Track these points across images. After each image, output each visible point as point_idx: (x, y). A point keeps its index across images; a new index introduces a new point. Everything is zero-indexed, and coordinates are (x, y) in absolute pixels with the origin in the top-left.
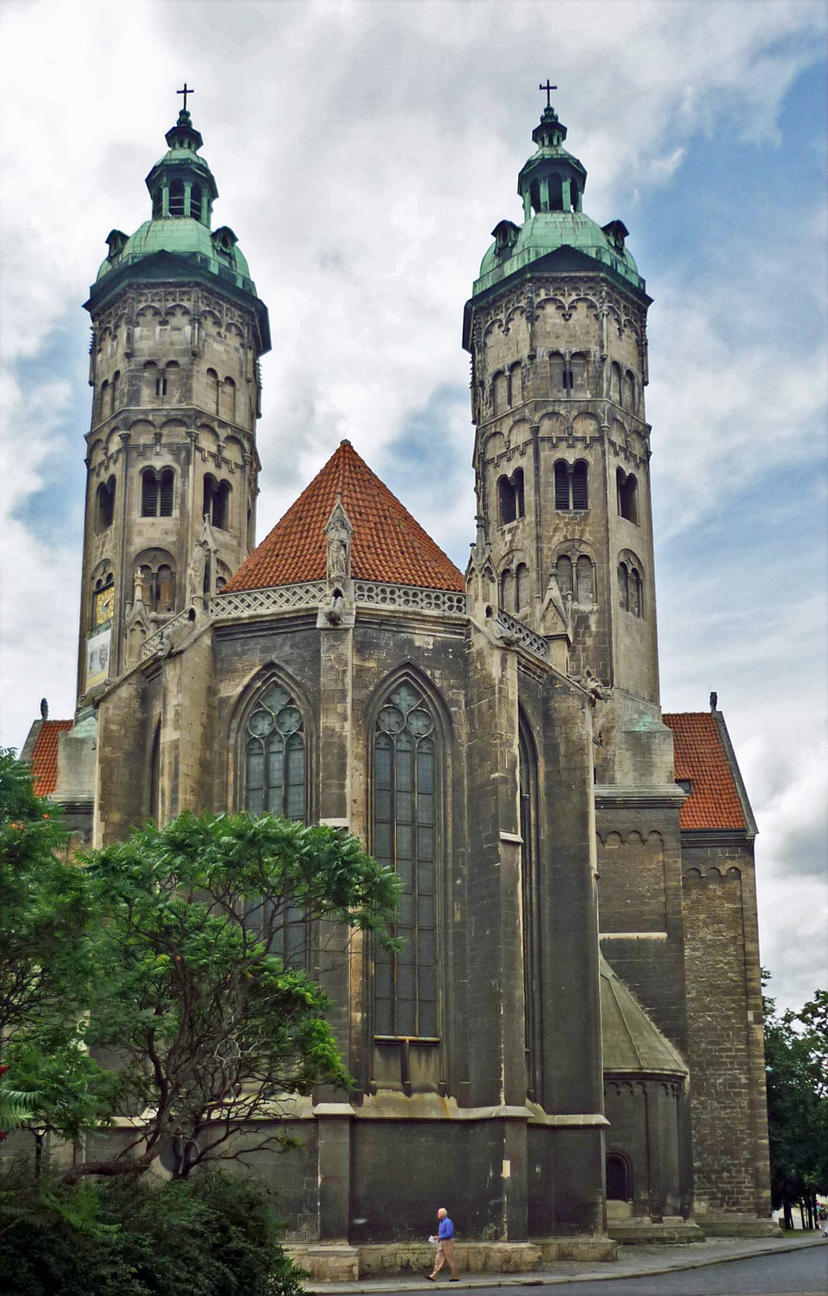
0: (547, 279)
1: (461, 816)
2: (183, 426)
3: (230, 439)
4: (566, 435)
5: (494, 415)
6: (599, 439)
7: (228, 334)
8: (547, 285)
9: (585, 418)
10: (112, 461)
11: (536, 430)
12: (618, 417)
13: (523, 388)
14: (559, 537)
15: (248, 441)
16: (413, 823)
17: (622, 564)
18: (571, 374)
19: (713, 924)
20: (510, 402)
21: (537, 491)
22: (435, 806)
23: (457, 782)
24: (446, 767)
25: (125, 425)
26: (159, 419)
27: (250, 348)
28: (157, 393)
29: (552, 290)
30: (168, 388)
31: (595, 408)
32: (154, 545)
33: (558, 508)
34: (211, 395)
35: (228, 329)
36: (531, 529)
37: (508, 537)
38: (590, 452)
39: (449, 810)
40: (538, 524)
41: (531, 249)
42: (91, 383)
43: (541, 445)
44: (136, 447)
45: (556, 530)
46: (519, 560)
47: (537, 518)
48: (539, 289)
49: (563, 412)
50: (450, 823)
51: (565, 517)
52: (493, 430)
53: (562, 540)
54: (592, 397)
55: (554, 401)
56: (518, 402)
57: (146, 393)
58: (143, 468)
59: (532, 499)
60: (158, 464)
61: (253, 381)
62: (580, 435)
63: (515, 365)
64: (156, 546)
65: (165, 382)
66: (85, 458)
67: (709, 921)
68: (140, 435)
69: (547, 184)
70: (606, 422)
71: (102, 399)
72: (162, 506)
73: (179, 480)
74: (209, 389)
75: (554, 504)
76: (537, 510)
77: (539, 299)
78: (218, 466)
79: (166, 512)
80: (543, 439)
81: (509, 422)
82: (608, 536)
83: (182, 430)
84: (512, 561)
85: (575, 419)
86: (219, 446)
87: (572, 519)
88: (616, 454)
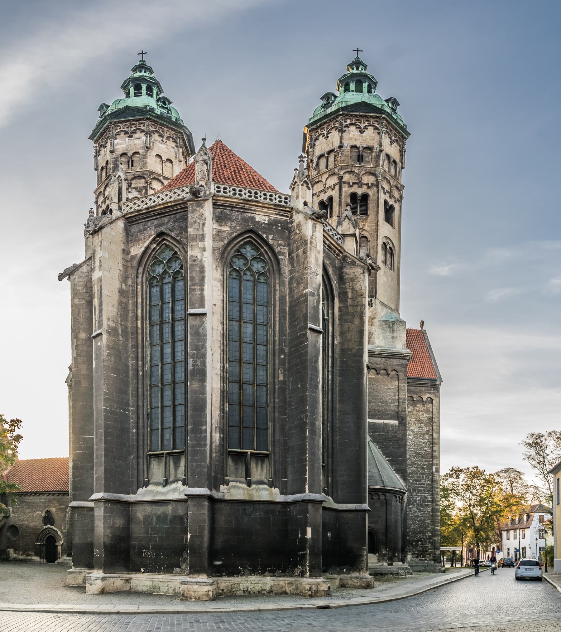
0: (352, 115)
1: (284, 318)
4: (358, 182)
7: (168, 141)
8: (352, 118)
9: (369, 175)
11: (341, 178)
13: (335, 161)
16: (254, 323)
17: (384, 243)
18: (362, 156)
19: (418, 423)
22: (268, 313)
23: (283, 299)
24: (275, 290)
27: (181, 147)
29: (354, 120)
35: (168, 138)
39: (277, 315)
41: (343, 102)
43: (343, 185)
48: (347, 119)
49: (357, 171)
50: (277, 322)
52: (317, 180)
55: (352, 166)
56: (331, 165)
59: (337, 209)
62: (365, 182)
63: (332, 151)
67: (416, 422)
69: (354, 83)
77: (346, 124)
80: (345, 183)
82: (378, 228)
85: (363, 175)
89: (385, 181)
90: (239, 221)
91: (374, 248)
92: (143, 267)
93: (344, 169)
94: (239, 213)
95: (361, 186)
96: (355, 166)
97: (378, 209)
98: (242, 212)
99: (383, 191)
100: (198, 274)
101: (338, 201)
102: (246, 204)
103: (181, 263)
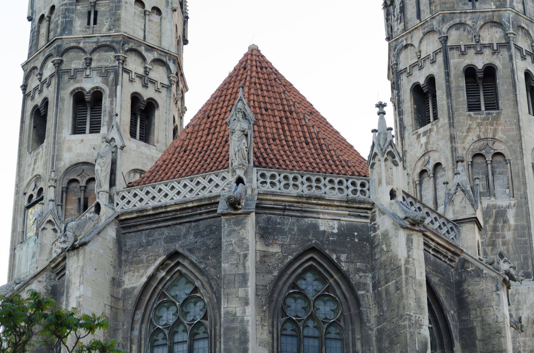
2: (111, 51)
3: (158, 61)
4: (474, 43)
5: (405, 29)
6: (507, 45)
9: (492, 27)
10: (45, 85)
12: (523, 25)
14: (472, 137)
15: (174, 63)
20: (419, 16)
21: (449, 95)
25: (57, 53)
26: (89, 47)
28: (89, 24)
30: (99, 18)
31: (500, 17)
32: (82, 160)
33: (470, 110)
34: (140, 23)
36: (444, 131)
37: (423, 140)
38: (498, 58)
40: (451, 125)
42: (30, 19)
43: (450, 53)
44: (68, 71)
45: (469, 130)
46: (434, 160)
47: (449, 120)
49: (469, 22)
51: (477, 118)
52: (404, 43)
53: (476, 139)
54: (497, 7)
55: (461, 13)
56: (426, 15)
57: (79, 24)
58: (74, 90)
59: (445, 102)
60: (88, 85)
61: (179, 10)
62: (486, 42)
64: (84, 160)
65: (96, 13)
66: (21, 84)
68: (71, 61)
70: (511, 29)
71: (39, 32)
72: (91, 124)
73: (108, 99)
74: (136, 18)
75: (466, 106)
76: (449, 113)
78: (145, 86)
79: (95, 129)
80: (452, 48)
81: (419, 34)
83: (112, 54)
84: (428, 162)
85: (481, 28)
86: (146, 68)
87: (484, 119)
88: (523, 58)
89: (520, 33)
90: (294, 235)
91: (519, 176)
92: (143, 311)
93: (447, 21)
94: (294, 220)
95: (481, 50)
96: (466, 12)
97: (516, 95)
98: (299, 217)
99: (519, 54)
100: (237, 345)
101: (444, 87)
102: (304, 203)
103: (204, 307)
